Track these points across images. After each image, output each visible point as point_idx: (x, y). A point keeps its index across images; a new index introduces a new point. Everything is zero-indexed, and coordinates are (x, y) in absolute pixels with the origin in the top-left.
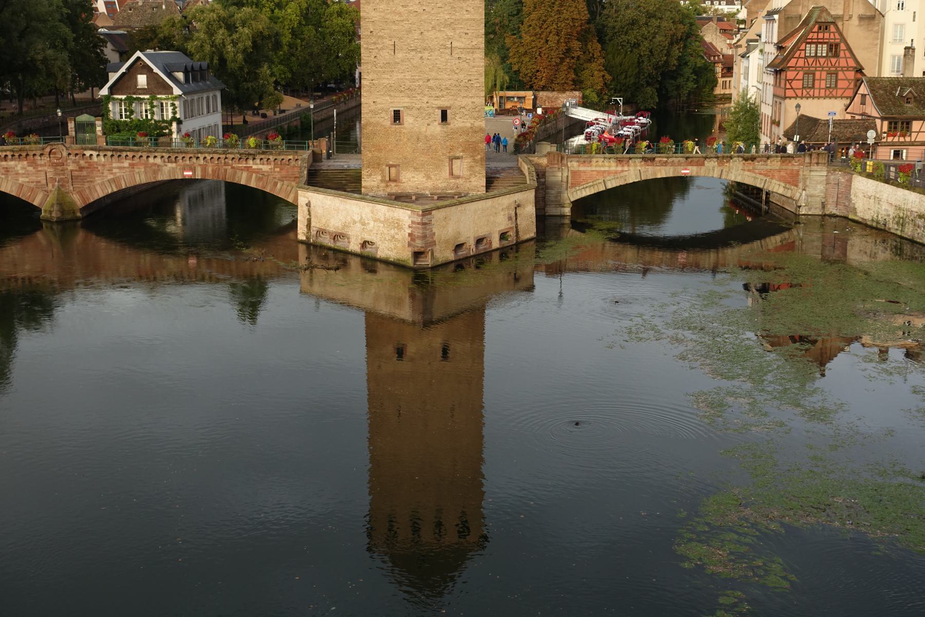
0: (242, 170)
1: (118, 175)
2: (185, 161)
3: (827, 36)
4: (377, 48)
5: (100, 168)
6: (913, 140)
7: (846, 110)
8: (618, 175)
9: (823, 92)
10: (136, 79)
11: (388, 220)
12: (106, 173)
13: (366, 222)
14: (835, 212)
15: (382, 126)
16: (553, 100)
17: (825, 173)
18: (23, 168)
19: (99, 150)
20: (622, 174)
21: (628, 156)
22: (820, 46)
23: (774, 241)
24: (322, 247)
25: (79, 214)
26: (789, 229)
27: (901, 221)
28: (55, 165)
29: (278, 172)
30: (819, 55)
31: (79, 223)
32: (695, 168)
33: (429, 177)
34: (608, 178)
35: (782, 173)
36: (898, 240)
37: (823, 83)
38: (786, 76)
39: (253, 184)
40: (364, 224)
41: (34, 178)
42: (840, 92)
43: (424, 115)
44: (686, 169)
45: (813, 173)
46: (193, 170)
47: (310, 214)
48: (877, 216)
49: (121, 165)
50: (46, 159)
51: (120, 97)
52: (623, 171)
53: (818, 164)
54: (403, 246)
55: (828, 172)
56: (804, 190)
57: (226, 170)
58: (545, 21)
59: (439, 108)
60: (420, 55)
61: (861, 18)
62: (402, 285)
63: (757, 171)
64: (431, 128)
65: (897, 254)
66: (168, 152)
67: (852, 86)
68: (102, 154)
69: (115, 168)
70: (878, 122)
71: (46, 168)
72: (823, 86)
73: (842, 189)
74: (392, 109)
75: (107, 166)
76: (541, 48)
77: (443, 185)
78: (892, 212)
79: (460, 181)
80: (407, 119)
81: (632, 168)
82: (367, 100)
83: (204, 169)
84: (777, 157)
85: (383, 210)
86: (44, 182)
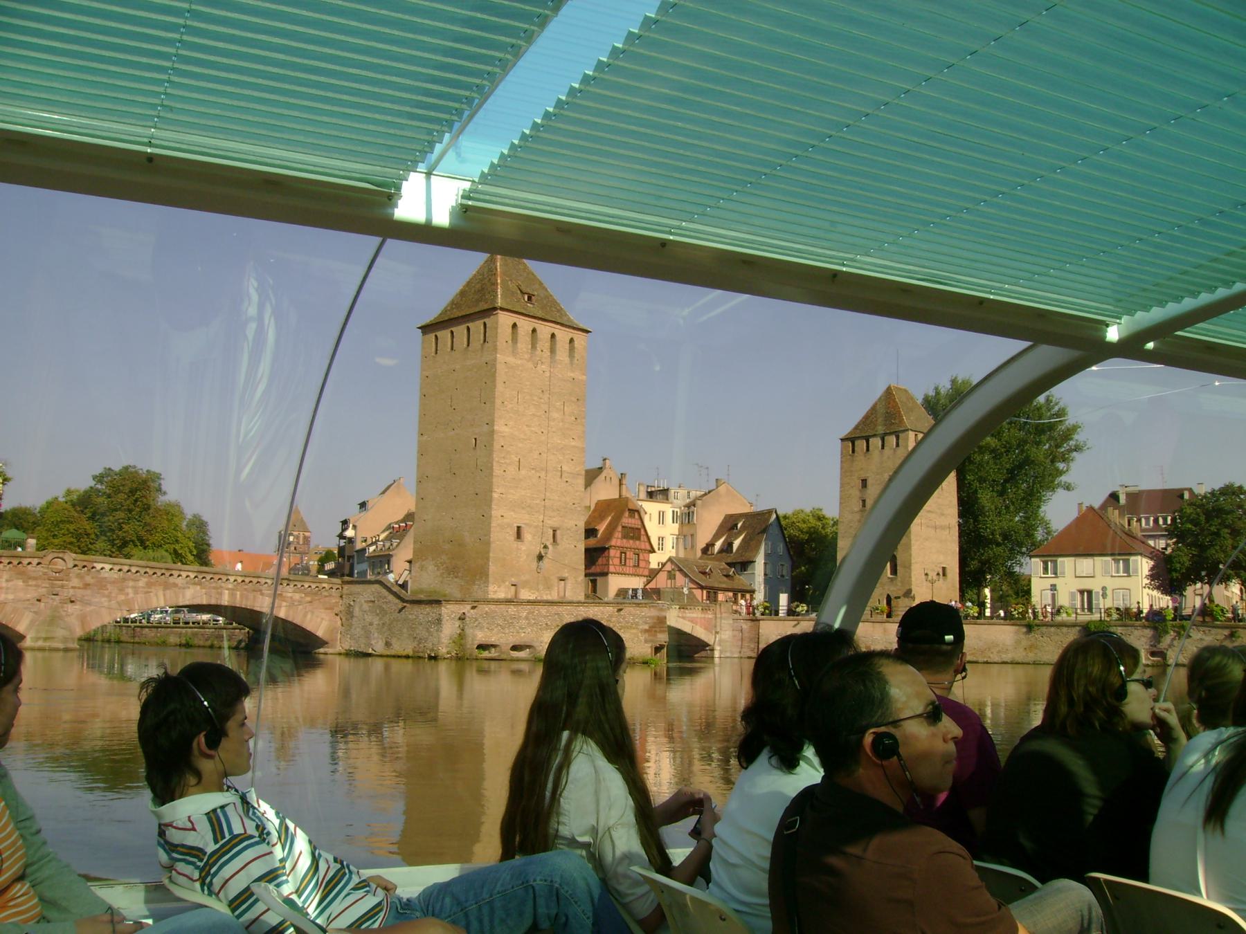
1: (131, 595)
4: (505, 463)
5: (108, 586)
17: (731, 622)
29: (311, 602)
41: (21, 595)
72: (631, 565)
73: (746, 635)
74: (516, 525)
80: (527, 536)
82: (496, 512)
83: (233, 595)
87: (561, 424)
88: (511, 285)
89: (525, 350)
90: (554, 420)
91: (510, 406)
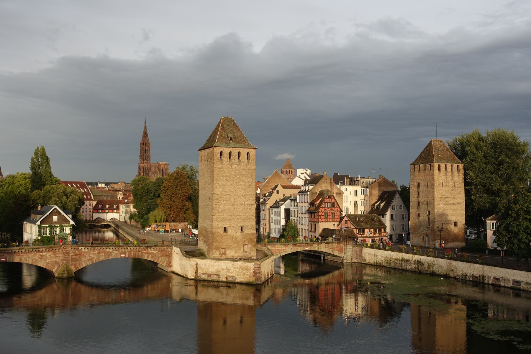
0: (145, 253)
1: (92, 257)
2: (122, 250)
3: (331, 200)
4: (219, 204)
5: (84, 254)
6: (366, 236)
7: (338, 226)
8: (285, 251)
9: (330, 219)
10: (53, 217)
11: (242, 267)
12: (87, 256)
13: (230, 269)
14: (355, 261)
15: (220, 233)
16: (176, 226)
18: (50, 255)
19: (85, 247)
20: (286, 250)
21: (288, 243)
22: (326, 203)
23: (336, 273)
24: (204, 280)
25: (74, 275)
26: (340, 268)
27: (389, 262)
28: (64, 254)
29: (160, 254)
30: (328, 206)
31: (73, 279)
32: (310, 247)
33: (236, 252)
34: (281, 252)
35: (338, 248)
36: (388, 269)
37: (330, 216)
38: (319, 214)
39: (150, 259)
40: (227, 269)
41: (54, 260)
42: (336, 220)
43: (235, 229)
44: (306, 248)
45: (348, 248)
46: (125, 253)
47: (197, 267)
48: (377, 261)
49: (94, 253)
50: (61, 251)
51: (46, 225)
52: (286, 249)
53: (349, 244)
54: (250, 277)
55: (352, 247)
56: (345, 254)
57: (139, 253)
58: (173, 193)
59: (240, 226)
60: (234, 207)
61: (337, 194)
62: (249, 293)
63: (330, 248)
64: (237, 234)
65: (388, 274)
66: (115, 246)
67: (339, 217)
68: (86, 248)
69: (92, 254)
70: (355, 230)
71: (60, 255)
72: (330, 218)
73: (358, 253)
75: (88, 253)
76: (171, 204)
77: (242, 255)
78: (383, 259)
79: (247, 253)
80: (229, 231)
81: (289, 248)
82: (215, 224)
83: (130, 253)
84: (336, 242)
85: (239, 264)
86: (59, 261)
87: (244, 186)
88: (224, 135)
89: (227, 161)
90: (241, 185)
91: (220, 183)
